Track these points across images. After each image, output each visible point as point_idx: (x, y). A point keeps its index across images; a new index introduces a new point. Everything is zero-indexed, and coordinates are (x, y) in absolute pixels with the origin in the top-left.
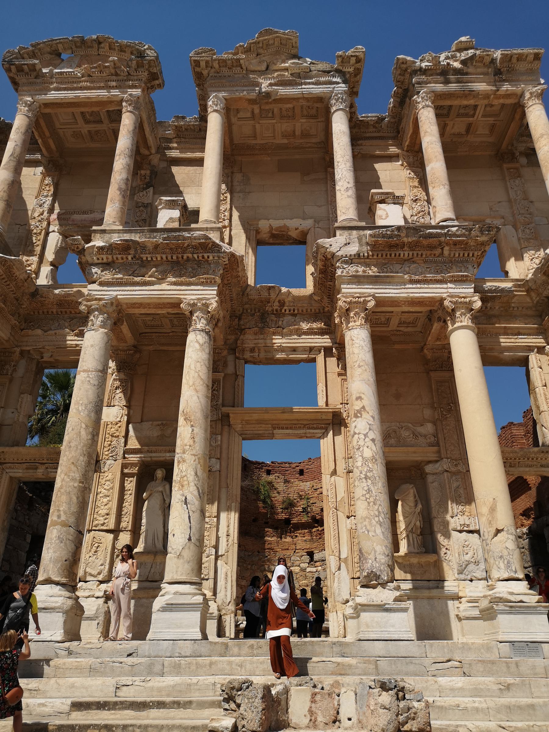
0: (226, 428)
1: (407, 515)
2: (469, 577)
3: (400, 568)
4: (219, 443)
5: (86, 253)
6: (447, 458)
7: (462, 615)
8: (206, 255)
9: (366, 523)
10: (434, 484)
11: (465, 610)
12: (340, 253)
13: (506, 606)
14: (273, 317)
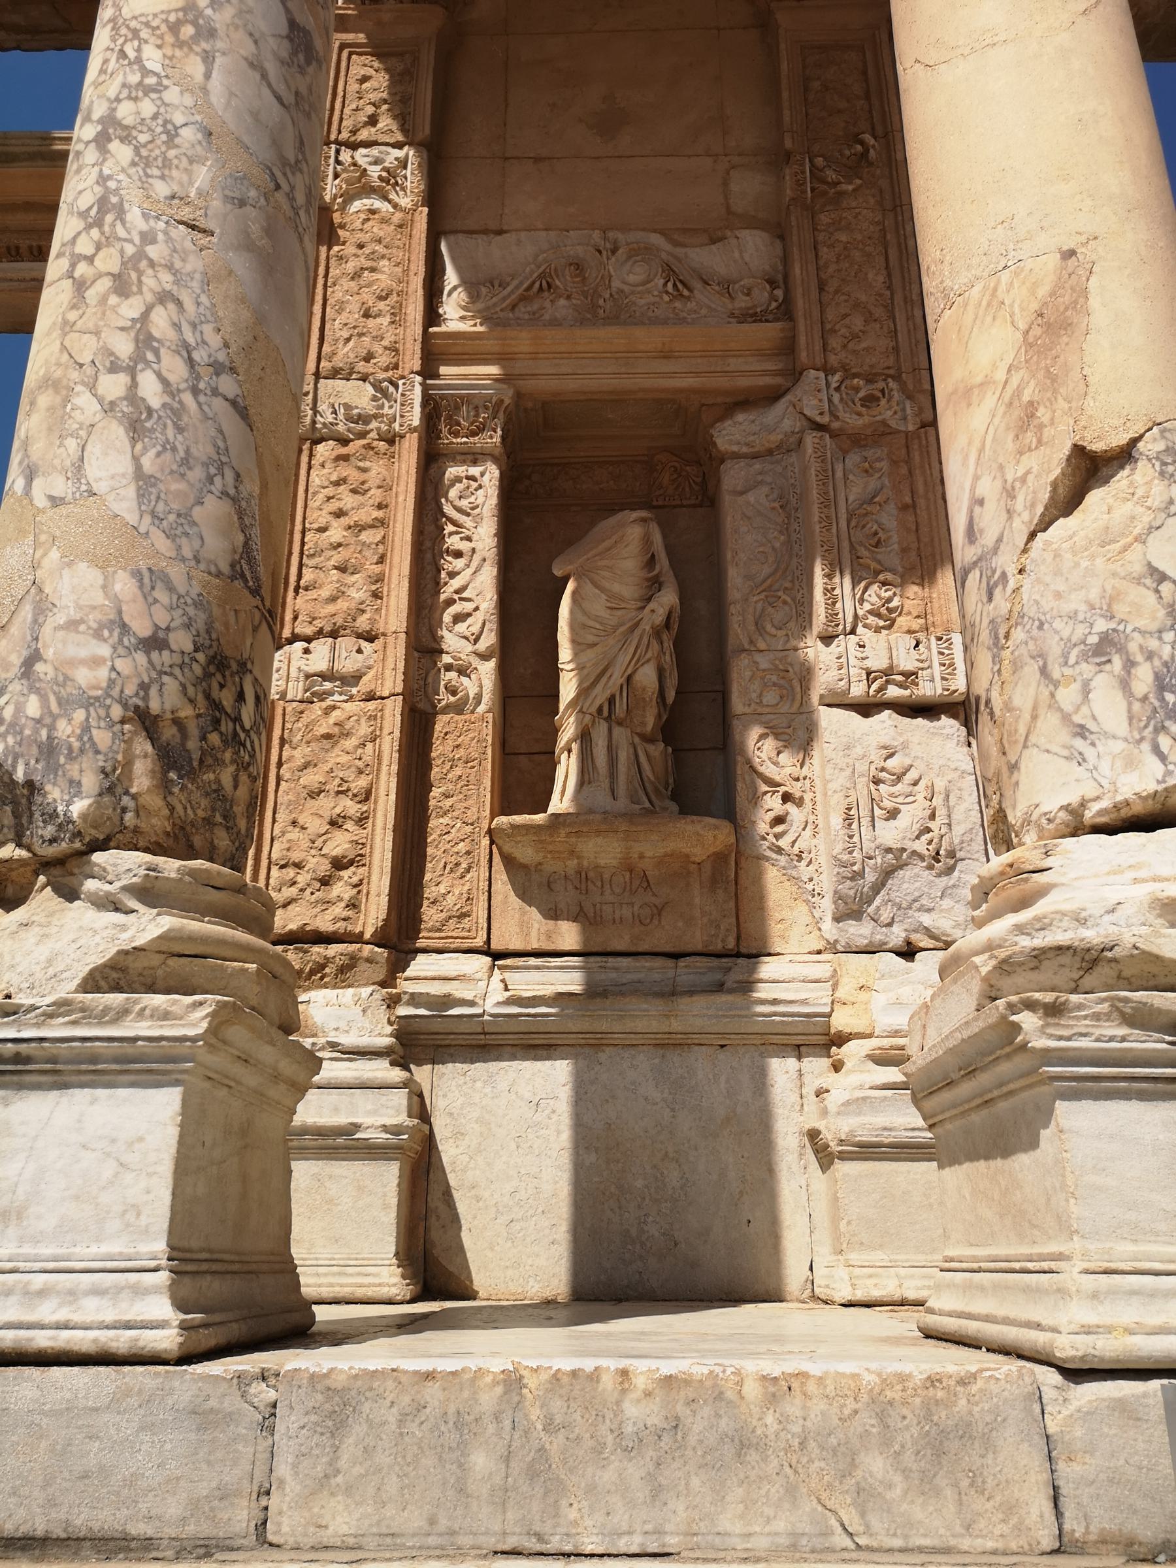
1: (591, 639)
2: (897, 936)
3: (524, 894)
6: (828, 371)
7: (835, 1129)
10: (751, 497)
11: (853, 1105)
13: (1139, 1019)
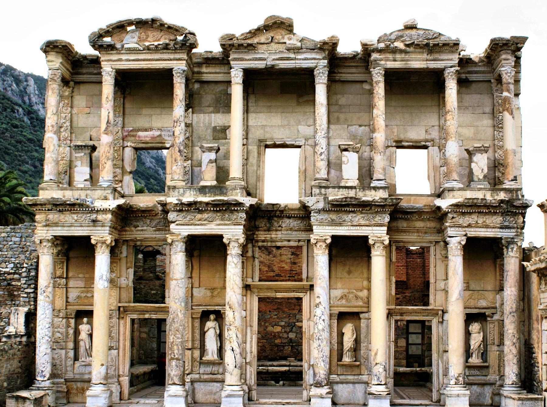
0: (249, 292)
4: (245, 300)
8: (236, 209)
9: (317, 360)
12: (313, 208)
14: (276, 219)
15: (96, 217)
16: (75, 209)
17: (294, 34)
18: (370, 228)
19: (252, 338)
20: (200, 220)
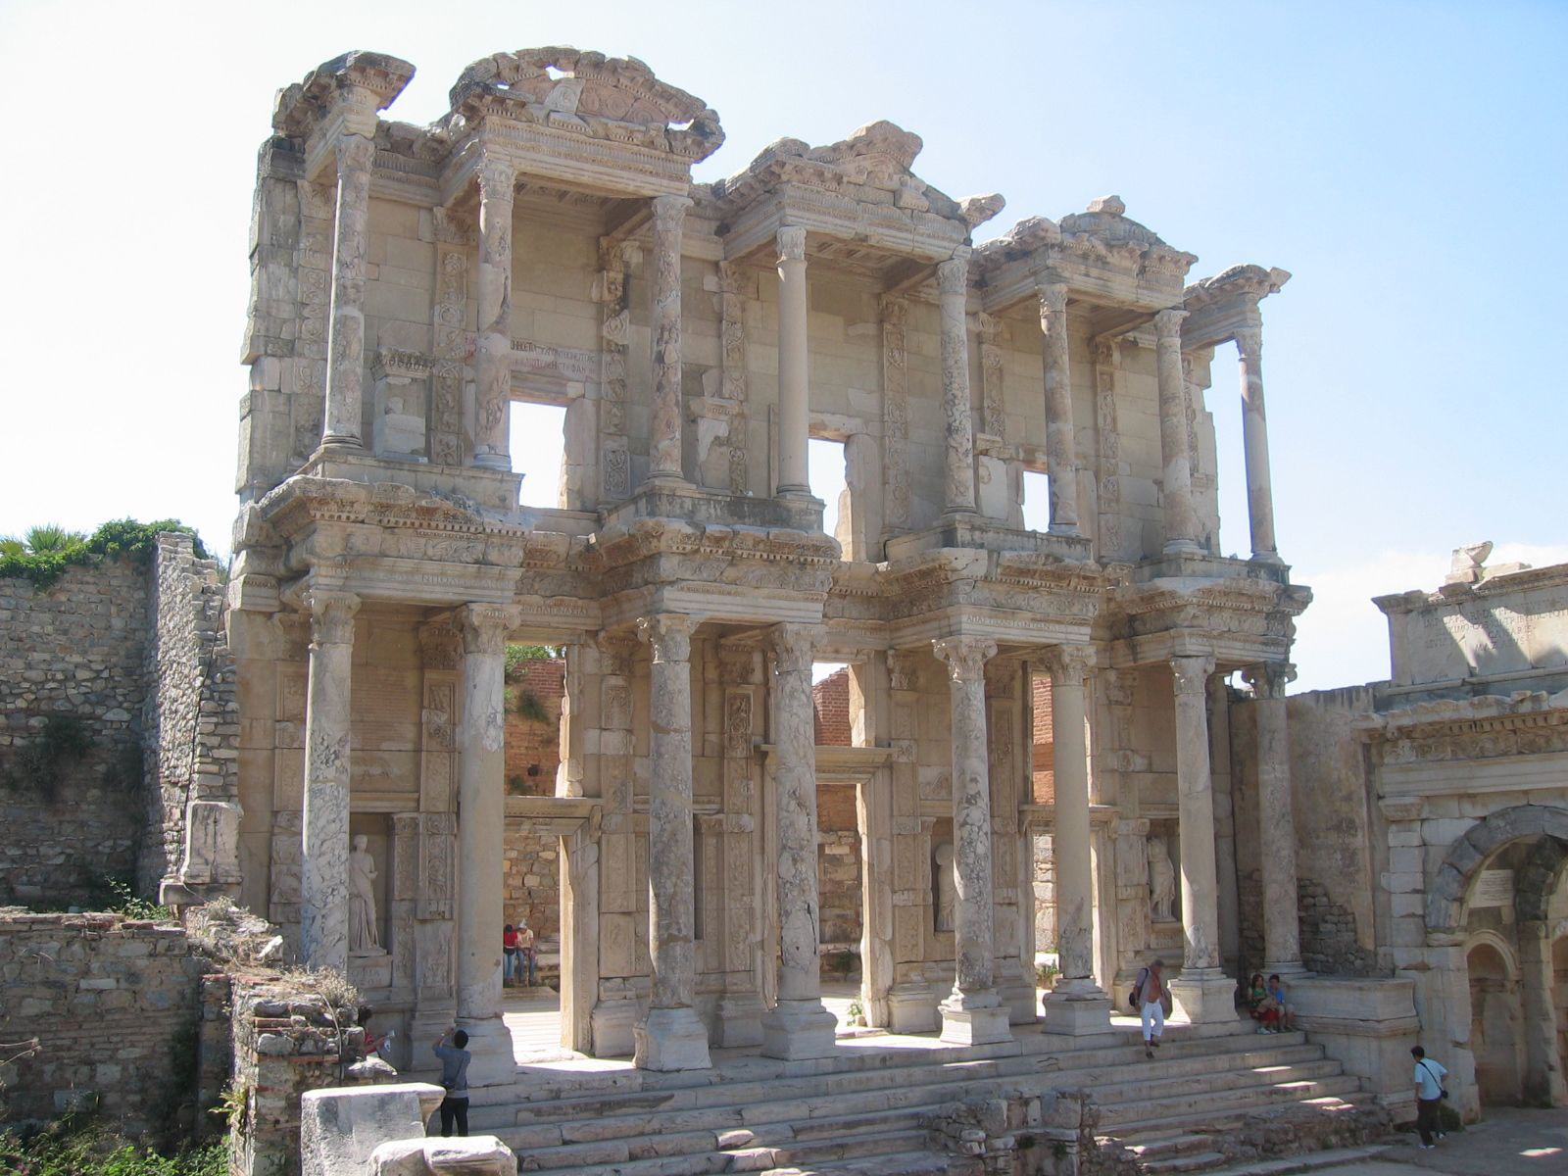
5: (663, 538)
8: (816, 559)
12: (965, 573)
15: (484, 554)
16: (433, 524)
17: (912, 175)
18: (1063, 628)
19: (765, 883)
20: (734, 583)
